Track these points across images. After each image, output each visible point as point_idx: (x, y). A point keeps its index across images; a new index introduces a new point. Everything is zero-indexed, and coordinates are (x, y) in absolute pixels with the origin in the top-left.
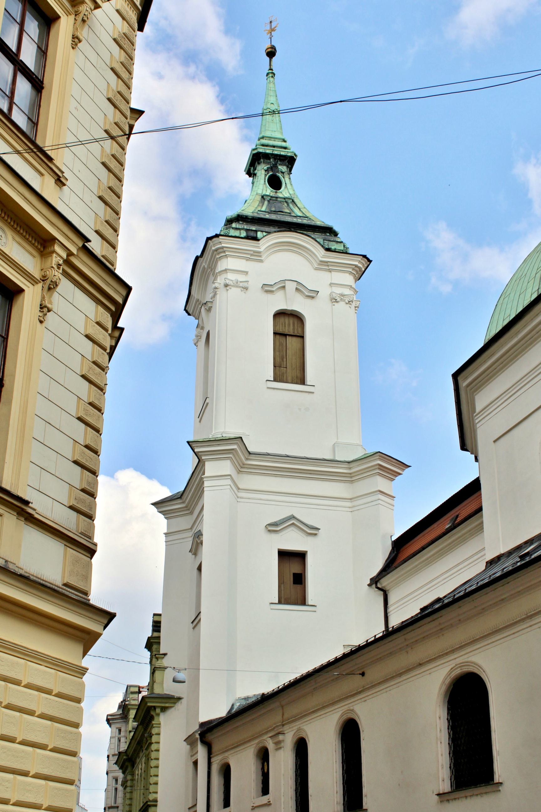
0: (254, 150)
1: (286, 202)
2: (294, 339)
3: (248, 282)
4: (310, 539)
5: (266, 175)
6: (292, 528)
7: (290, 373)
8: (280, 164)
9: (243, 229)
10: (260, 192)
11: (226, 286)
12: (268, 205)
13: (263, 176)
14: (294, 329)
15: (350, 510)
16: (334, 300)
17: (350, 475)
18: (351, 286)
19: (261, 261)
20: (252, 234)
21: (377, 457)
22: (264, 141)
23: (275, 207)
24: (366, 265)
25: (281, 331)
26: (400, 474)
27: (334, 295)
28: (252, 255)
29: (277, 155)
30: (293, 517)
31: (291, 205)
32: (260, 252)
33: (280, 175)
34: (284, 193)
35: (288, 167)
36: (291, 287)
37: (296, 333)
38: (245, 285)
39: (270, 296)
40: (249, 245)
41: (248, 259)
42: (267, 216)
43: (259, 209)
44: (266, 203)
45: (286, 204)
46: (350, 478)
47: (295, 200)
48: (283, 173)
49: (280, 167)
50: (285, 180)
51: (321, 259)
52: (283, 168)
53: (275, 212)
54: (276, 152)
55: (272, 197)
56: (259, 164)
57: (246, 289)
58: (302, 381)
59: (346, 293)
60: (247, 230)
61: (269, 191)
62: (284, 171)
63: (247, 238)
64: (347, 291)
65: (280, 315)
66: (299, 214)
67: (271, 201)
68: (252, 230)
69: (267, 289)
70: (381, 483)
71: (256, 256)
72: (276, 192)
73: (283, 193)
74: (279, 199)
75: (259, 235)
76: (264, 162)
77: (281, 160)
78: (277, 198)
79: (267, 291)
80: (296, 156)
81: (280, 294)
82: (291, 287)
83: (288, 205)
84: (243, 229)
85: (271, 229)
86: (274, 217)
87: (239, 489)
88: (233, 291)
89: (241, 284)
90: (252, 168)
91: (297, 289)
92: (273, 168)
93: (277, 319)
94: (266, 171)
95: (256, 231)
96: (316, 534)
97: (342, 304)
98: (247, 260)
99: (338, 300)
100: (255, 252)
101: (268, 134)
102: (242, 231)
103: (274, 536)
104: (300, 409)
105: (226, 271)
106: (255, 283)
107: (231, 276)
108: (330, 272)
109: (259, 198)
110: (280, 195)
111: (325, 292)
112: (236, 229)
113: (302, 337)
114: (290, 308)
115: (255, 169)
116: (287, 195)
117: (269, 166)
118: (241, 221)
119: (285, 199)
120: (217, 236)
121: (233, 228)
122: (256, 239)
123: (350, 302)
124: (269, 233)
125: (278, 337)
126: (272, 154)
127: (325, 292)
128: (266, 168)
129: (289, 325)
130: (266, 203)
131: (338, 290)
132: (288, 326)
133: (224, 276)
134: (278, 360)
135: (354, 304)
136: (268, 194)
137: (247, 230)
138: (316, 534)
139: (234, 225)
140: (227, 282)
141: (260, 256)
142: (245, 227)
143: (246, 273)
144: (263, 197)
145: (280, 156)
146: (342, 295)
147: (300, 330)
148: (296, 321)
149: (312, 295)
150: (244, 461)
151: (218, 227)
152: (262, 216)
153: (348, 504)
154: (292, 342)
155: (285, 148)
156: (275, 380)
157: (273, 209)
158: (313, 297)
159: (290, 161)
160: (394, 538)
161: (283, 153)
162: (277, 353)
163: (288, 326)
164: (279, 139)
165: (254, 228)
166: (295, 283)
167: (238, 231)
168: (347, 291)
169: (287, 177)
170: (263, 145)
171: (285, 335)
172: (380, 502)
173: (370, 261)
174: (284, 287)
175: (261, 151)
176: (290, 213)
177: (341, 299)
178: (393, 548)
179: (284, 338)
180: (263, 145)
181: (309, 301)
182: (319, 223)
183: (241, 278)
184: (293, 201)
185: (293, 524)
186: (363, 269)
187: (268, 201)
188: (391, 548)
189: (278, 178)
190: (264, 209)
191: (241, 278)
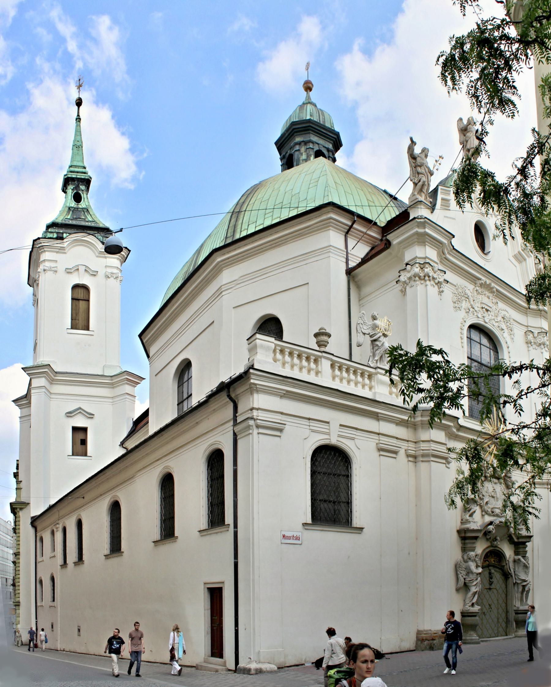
0: (65, 175)
1: (83, 211)
2: (84, 302)
3: (57, 267)
4: (89, 420)
5: (72, 193)
6: (80, 414)
7: (81, 322)
8: (81, 185)
9: (55, 232)
10: (68, 205)
11: (45, 270)
12: (72, 214)
13: (71, 193)
14: (84, 296)
15: (112, 404)
16: (107, 277)
17: (112, 384)
18: (118, 268)
19: (65, 253)
20: (60, 235)
21: (125, 374)
22: (72, 169)
23: (76, 215)
24: (127, 254)
25: (76, 297)
26: (139, 383)
27: (107, 273)
28: (59, 249)
29: (79, 178)
30: (80, 408)
31: (86, 213)
32: (64, 247)
33: (80, 192)
34: (82, 205)
35: (86, 186)
36: (82, 269)
37: (85, 298)
38: (55, 269)
39: (70, 275)
40: (57, 244)
41: (57, 252)
42: (71, 222)
43: (66, 217)
44: (71, 212)
45: (83, 213)
46: (112, 386)
47: (89, 210)
48: (83, 190)
49: (81, 187)
50: (84, 195)
51: (100, 250)
52: (83, 187)
53: (76, 219)
54: (78, 177)
55: (75, 208)
56: (69, 185)
57: (56, 271)
58: (87, 328)
59: (114, 272)
60: (57, 233)
61: (73, 204)
62: (83, 189)
63: (57, 238)
64: (115, 271)
65: (76, 287)
66: (90, 219)
67: (74, 211)
68: (60, 233)
69: (68, 271)
70: (128, 388)
71: (62, 250)
72: (78, 205)
73: (82, 205)
74: (79, 210)
75: (65, 235)
76: (71, 184)
77: (81, 182)
78: (78, 208)
79: (68, 273)
80: (91, 178)
81: (76, 273)
82: (82, 269)
83: (84, 213)
84: (55, 232)
85: (73, 231)
86: (74, 222)
87: (51, 393)
88: (49, 273)
89: (53, 269)
90: (65, 188)
91: (85, 270)
92: (77, 188)
93: (74, 290)
94: (72, 190)
95: (63, 233)
96: (92, 418)
97: (112, 278)
98: (57, 253)
99: (110, 276)
100: (61, 247)
101: (75, 163)
102: (54, 234)
103: (70, 419)
104: (85, 345)
105: (44, 260)
106: (61, 268)
107: (47, 264)
108: (106, 258)
109: (67, 209)
110: (80, 207)
111: (102, 273)
112: (51, 232)
113: (88, 301)
114: (81, 283)
115: (66, 189)
116: (84, 206)
117: (74, 186)
118: (55, 226)
119: (82, 209)
120: (39, 238)
121: (49, 232)
122: (62, 238)
123: (117, 278)
124: (70, 234)
125: (74, 301)
126: (76, 178)
127: (102, 273)
128: (72, 188)
129: (81, 293)
130: (71, 212)
131: (110, 270)
132: (80, 294)
133: (43, 264)
134: (74, 315)
135: (119, 279)
136: (72, 206)
137: (57, 233)
138: (92, 418)
139: (50, 230)
140: (45, 268)
141: (64, 250)
142: (57, 231)
143: (56, 261)
144: (69, 208)
145: (81, 179)
146: (112, 273)
147: (87, 296)
148: (85, 290)
149: (94, 274)
150: (53, 376)
151: (39, 232)
152: (67, 222)
153: (111, 400)
154: (82, 304)
155: (85, 173)
156: (72, 328)
157: (75, 217)
158: (95, 275)
159: (87, 182)
160: (134, 420)
161: (83, 177)
162: (74, 311)
163: (80, 294)
164: (81, 166)
165: (61, 232)
166: (85, 267)
167: (52, 234)
168: (115, 271)
169: (85, 193)
170: (71, 172)
171: (79, 300)
172: (127, 399)
173: (130, 251)
174: (78, 269)
175: (69, 176)
176: (85, 219)
177: (112, 276)
178: (133, 425)
179: (78, 302)
180: (71, 172)
181: (92, 278)
182: (101, 226)
183: (53, 265)
184: (87, 210)
185: (80, 412)
186: (126, 256)
187: (73, 211)
188: (132, 425)
189: (80, 194)
190: (69, 217)
191: (53, 265)
